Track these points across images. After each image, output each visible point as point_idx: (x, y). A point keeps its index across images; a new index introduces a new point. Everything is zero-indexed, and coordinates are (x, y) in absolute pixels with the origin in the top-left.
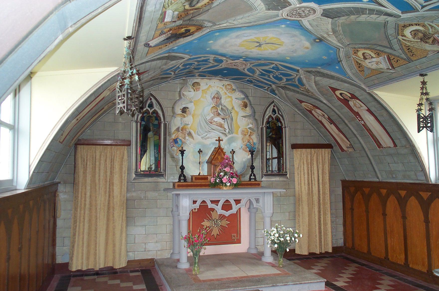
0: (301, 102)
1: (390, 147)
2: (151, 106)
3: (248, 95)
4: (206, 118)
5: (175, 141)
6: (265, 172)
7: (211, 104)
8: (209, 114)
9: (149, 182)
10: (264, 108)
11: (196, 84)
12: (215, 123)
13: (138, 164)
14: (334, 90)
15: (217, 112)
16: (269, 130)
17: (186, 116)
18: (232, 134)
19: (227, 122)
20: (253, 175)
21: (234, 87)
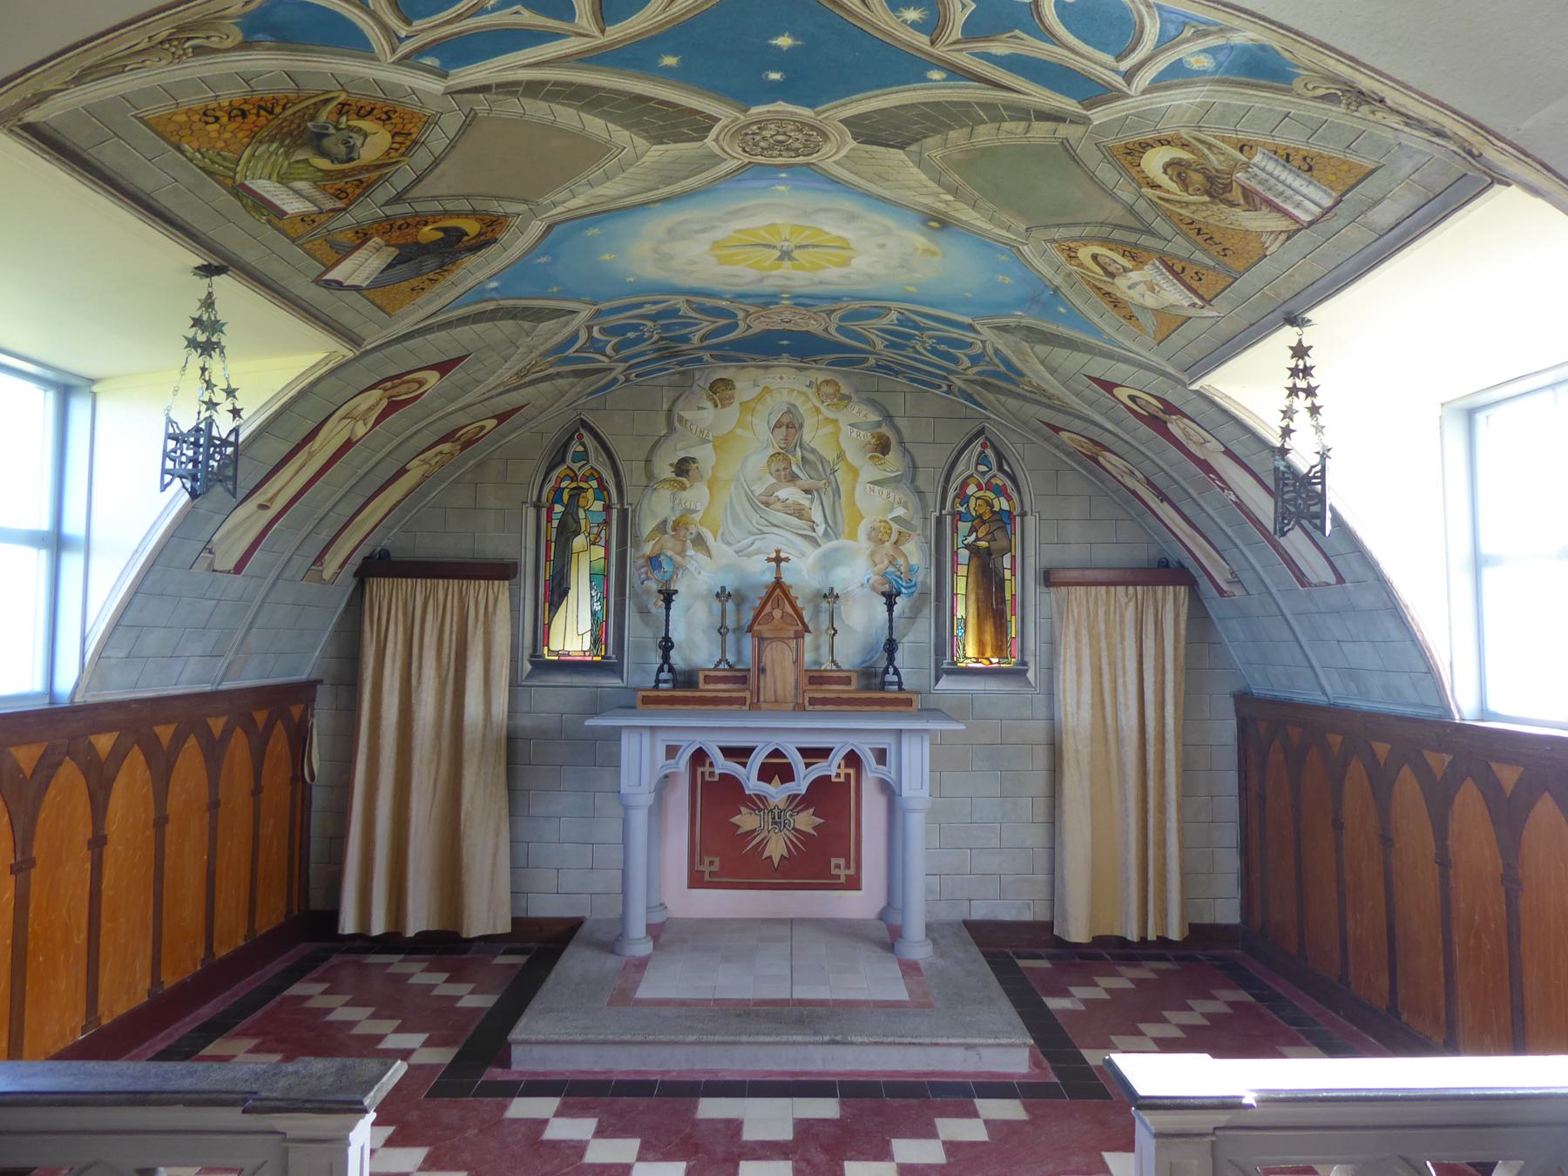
0: (1057, 430)
1: (1329, 584)
2: (584, 456)
3: (892, 412)
4: (752, 492)
5: (654, 562)
6: (948, 664)
7: (768, 446)
8: (760, 479)
9: (571, 687)
10: (945, 455)
11: (720, 384)
12: (779, 505)
13: (541, 634)
14: (1109, 386)
15: (787, 471)
17: (688, 485)
18: (837, 538)
19: (819, 502)
20: (891, 670)
21: (844, 390)
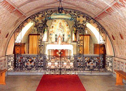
16: (74, 31)
